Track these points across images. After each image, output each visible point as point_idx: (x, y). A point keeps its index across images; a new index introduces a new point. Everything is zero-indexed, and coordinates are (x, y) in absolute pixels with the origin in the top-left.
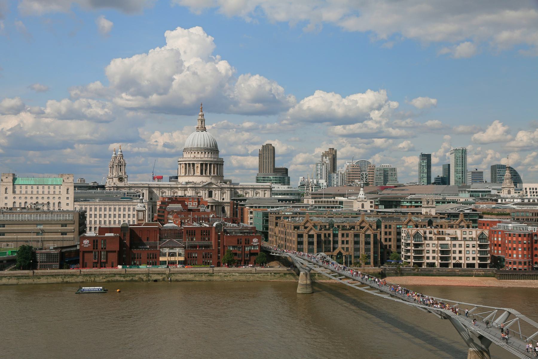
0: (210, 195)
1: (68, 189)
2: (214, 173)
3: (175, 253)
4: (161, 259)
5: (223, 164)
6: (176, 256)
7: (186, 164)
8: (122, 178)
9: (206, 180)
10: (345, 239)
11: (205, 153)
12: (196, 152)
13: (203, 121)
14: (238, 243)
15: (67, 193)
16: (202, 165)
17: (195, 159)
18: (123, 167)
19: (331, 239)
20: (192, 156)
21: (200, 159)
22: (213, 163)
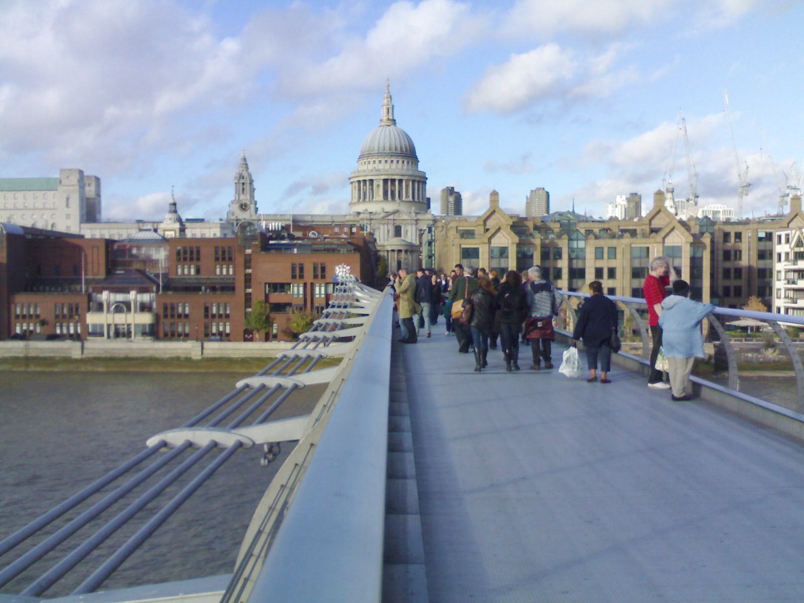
0: (398, 232)
1: (68, 199)
2: (407, 196)
3: (128, 305)
4: (92, 319)
5: (426, 183)
6: (129, 309)
7: (359, 182)
8: (246, 205)
9: (390, 207)
10: (605, 264)
11: (392, 161)
12: (377, 162)
13: (390, 110)
14: (294, 277)
15: (67, 206)
16: (385, 181)
17: (374, 173)
18: (247, 187)
19: (563, 264)
20: (370, 167)
21: (382, 172)
22: (405, 178)
